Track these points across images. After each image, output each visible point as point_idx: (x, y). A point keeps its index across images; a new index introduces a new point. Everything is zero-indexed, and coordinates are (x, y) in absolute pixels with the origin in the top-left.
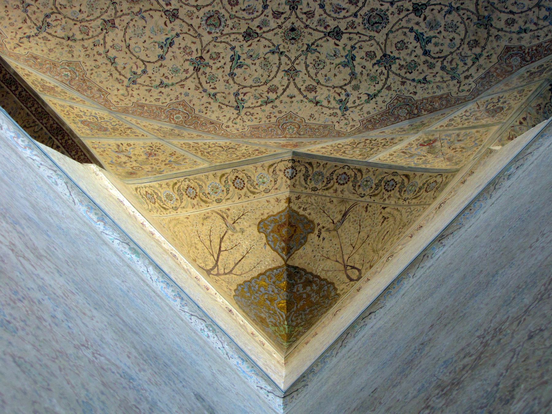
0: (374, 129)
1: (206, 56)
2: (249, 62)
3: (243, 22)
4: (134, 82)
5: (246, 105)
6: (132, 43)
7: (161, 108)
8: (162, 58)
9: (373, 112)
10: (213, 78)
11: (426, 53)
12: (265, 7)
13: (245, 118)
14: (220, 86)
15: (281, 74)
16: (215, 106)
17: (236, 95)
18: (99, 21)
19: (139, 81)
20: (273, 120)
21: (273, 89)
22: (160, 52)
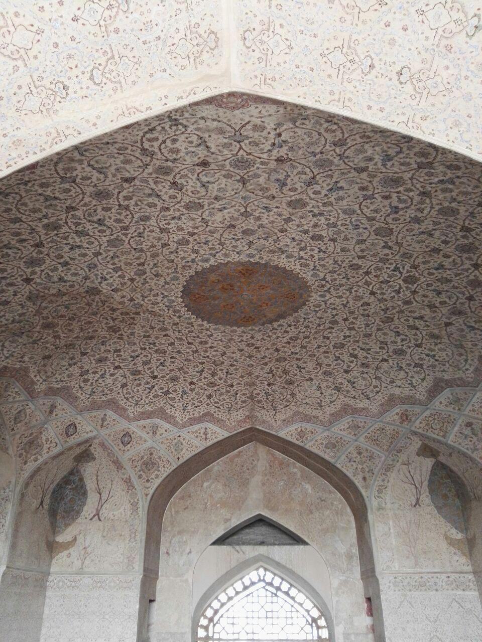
0: (435, 397)
1: (337, 385)
2: (355, 380)
4: (322, 406)
6: (306, 394)
8: (322, 393)
9: (429, 386)
10: (347, 392)
11: (436, 360)
12: (343, 361)
13: (375, 402)
15: (374, 380)
16: (358, 401)
17: (363, 394)
18: (289, 396)
21: (375, 387)
22: (319, 392)
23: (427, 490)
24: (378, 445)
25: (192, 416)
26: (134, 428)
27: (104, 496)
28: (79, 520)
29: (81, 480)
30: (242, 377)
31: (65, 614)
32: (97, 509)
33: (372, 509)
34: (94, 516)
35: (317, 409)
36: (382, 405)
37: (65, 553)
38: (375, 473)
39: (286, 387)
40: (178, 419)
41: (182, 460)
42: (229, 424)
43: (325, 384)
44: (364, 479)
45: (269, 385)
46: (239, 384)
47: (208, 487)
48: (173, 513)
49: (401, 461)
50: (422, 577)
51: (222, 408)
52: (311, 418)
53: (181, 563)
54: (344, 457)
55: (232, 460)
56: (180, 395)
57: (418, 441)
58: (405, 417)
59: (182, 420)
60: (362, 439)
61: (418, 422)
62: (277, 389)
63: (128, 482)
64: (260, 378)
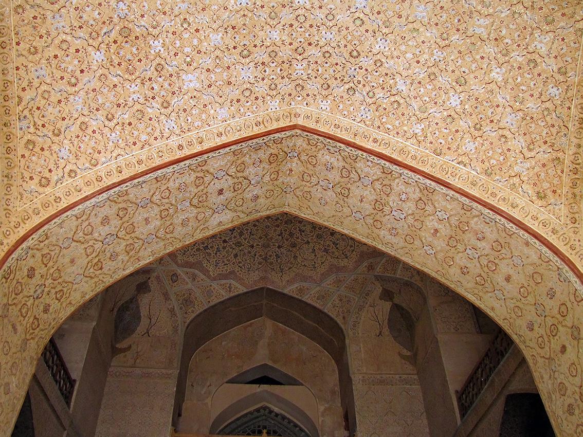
2: (338, 242)
3: (328, 232)
5: (348, 255)
7: (327, 271)
8: (315, 256)
10: (333, 253)
14: (336, 253)
15: (350, 240)
17: (343, 254)
19: (316, 266)
20: (358, 256)
21: (351, 246)
22: (313, 254)
23: (387, 326)
24: (353, 291)
25: (221, 272)
26: (179, 271)
27: (153, 321)
28: (134, 335)
29: (138, 307)
30: (261, 238)
31: (120, 392)
32: (147, 329)
33: (348, 336)
34: (145, 333)
35: (312, 270)
36: (356, 261)
37: (122, 355)
38: (351, 311)
39: (291, 250)
40: (211, 273)
41: (212, 304)
42: (247, 282)
43: (318, 246)
44: (344, 318)
45: (278, 247)
46: (258, 245)
47: (226, 342)
48: (197, 360)
49: (369, 303)
50: (382, 377)
51: (243, 268)
52: (307, 279)
53: (203, 392)
54: (330, 304)
55: (245, 328)
56: (215, 252)
57: (380, 286)
58: (371, 268)
59: (214, 275)
60: (342, 289)
61: (378, 268)
62: (285, 251)
63: (172, 311)
64: (273, 241)
